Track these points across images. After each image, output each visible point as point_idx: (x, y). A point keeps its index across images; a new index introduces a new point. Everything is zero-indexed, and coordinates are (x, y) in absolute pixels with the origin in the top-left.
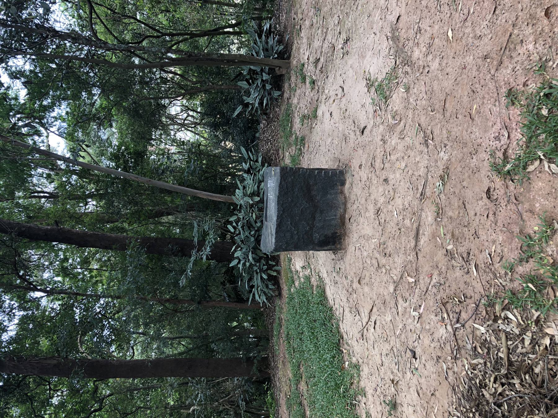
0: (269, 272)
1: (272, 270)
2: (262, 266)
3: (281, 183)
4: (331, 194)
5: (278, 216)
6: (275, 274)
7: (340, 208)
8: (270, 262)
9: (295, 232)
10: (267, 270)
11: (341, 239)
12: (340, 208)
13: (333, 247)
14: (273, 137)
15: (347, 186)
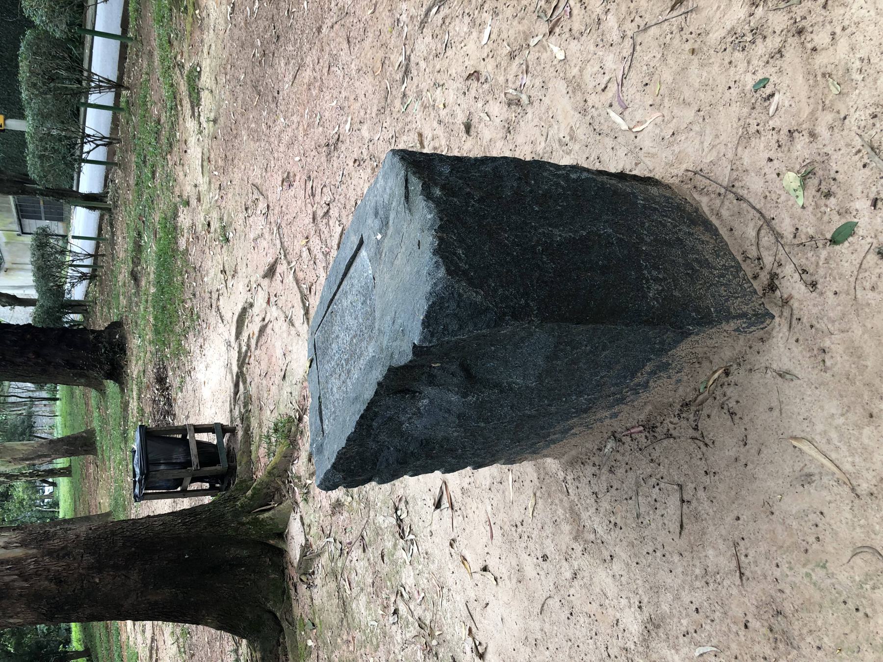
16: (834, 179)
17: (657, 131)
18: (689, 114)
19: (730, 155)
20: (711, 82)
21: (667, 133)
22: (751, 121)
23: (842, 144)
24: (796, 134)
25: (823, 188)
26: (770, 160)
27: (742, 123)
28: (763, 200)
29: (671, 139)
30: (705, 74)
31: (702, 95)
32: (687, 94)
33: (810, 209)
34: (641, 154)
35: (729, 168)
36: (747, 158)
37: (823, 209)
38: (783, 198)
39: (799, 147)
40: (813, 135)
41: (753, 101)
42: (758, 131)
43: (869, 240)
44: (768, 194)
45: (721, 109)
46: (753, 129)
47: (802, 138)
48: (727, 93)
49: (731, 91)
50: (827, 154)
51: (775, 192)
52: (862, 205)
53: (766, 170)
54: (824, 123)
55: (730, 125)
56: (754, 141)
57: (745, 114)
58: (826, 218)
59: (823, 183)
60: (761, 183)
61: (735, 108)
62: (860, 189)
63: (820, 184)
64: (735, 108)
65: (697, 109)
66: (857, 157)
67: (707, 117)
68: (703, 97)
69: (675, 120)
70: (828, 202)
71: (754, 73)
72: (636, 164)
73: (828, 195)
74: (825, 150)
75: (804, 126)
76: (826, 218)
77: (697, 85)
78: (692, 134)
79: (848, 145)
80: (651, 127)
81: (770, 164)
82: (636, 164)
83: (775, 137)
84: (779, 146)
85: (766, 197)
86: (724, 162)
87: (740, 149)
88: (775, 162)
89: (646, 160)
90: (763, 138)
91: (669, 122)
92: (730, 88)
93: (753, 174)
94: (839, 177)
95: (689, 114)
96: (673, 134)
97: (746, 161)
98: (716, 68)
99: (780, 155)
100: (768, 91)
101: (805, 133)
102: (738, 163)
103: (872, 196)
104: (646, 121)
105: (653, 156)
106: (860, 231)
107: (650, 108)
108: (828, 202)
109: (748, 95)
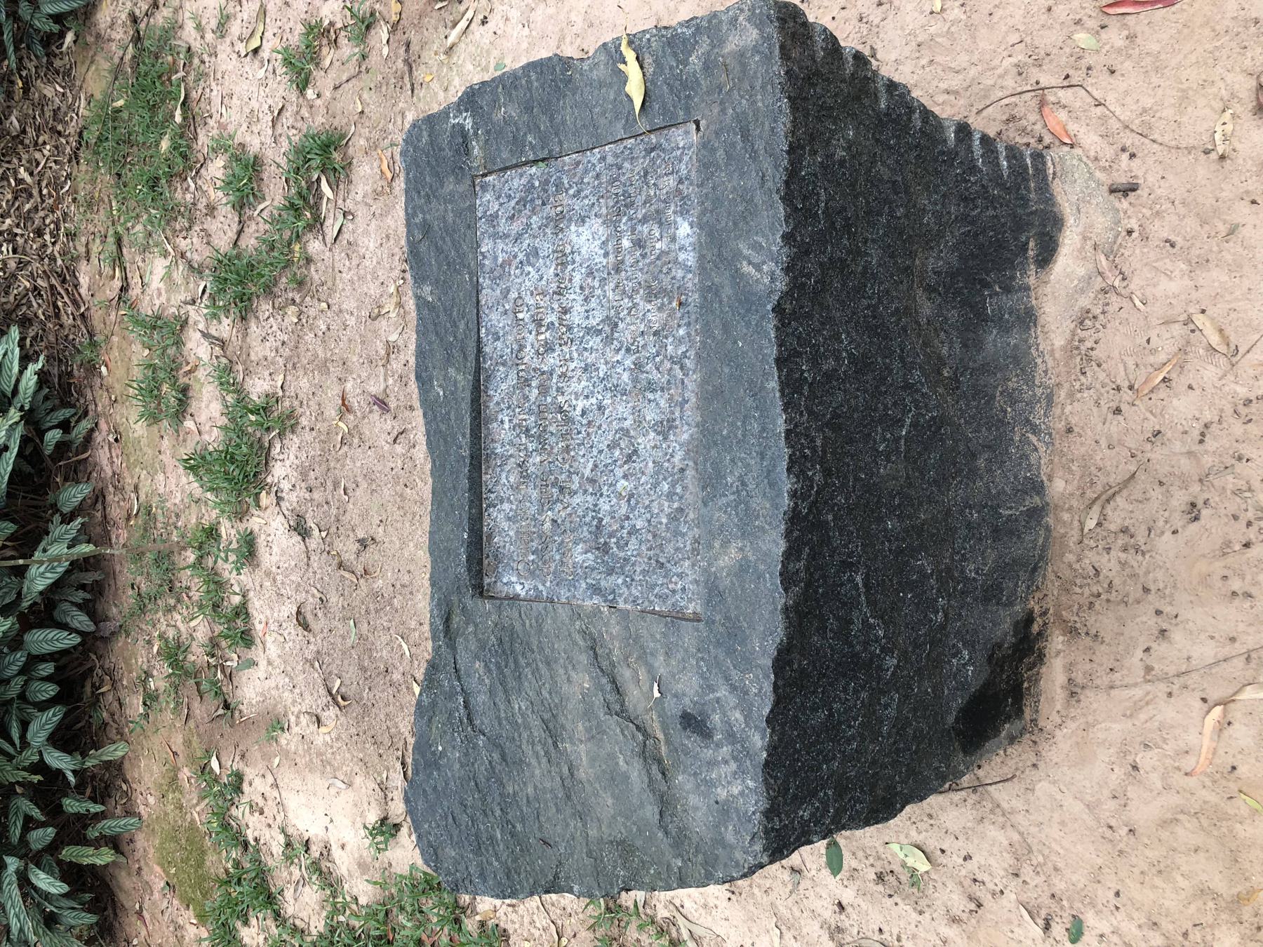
0: (70, 853)
1: (85, 842)
2: (16, 832)
3: (792, 175)
4: (1006, 330)
5: (794, 519)
6: (103, 857)
7: (1035, 430)
8: (72, 805)
9: (891, 662)
10: (53, 847)
11: (1041, 657)
12: (1035, 430)
13: (1018, 724)
14: (28, 217)
15: (1069, 261)
16: (890, 896)
17: (1170, 748)
18: (1145, 811)
19: (1019, 819)
20: (1158, 881)
21: (1146, 760)
22: (1039, 880)
23: (921, 933)
24: (973, 906)
25: (890, 879)
26: (967, 858)
27: (1049, 868)
28: (928, 811)
29: (1130, 758)
30: (1182, 883)
31: (1152, 854)
32: (1186, 834)
33: (881, 850)
34: (1163, 688)
35: (1005, 805)
36: (995, 834)
37: (871, 860)
38: (913, 833)
39: (955, 897)
40: (955, 920)
41: (1065, 903)
42: (1017, 875)
43: (813, 872)
44: (932, 822)
45: (1100, 861)
46: (1027, 872)
47: (962, 908)
48: (1115, 886)
49: (1111, 894)
50: (921, 913)
51: (927, 831)
52: (847, 896)
53: (960, 843)
54: (958, 940)
55: (1061, 851)
56: (1009, 859)
57: (1056, 880)
58: (860, 854)
59: (895, 883)
60: (949, 825)
61: (1080, 878)
62: (863, 905)
63: (897, 879)
64: (1080, 878)
65: (1139, 831)
66: (895, 932)
67: (1108, 833)
68: (1148, 852)
69: (1159, 785)
70: (873, 870)
71: (1101, 936)
72: (1149, 669)
73: (880, 877)
74: (927, 915)
75: (973, 921)
76: (860, 854)
77: (1181, 860)
78: (1106, 793)
79: (914, 936)
80: (1192, 738)
81: (964, 853)
82: (1149, 669)
83: (991, 886)
84: (975, 880)
85: (930, 816)
86: (1018, 804)
87: (1016, 837)
88: (961, 861)
89: (1138, 693)
90: (1002, 873)
91: (1164, 777)
92: (1117, 894)
93: (969, 824)
94: (890, 902)
95: (1145, 811)
96: (1135, 768)
97: (993, 832)
98: (1171, 902)
99: (964, 872)
100: (1058, 930)
101: (964, 916)
102: (1001, 819)
103: (849, 910)
104: (1211, 738)
105: (1137, 707)
106: (826, 872)
107: (1231, 761)
108: (873, 870)
109: (1080, 905)
